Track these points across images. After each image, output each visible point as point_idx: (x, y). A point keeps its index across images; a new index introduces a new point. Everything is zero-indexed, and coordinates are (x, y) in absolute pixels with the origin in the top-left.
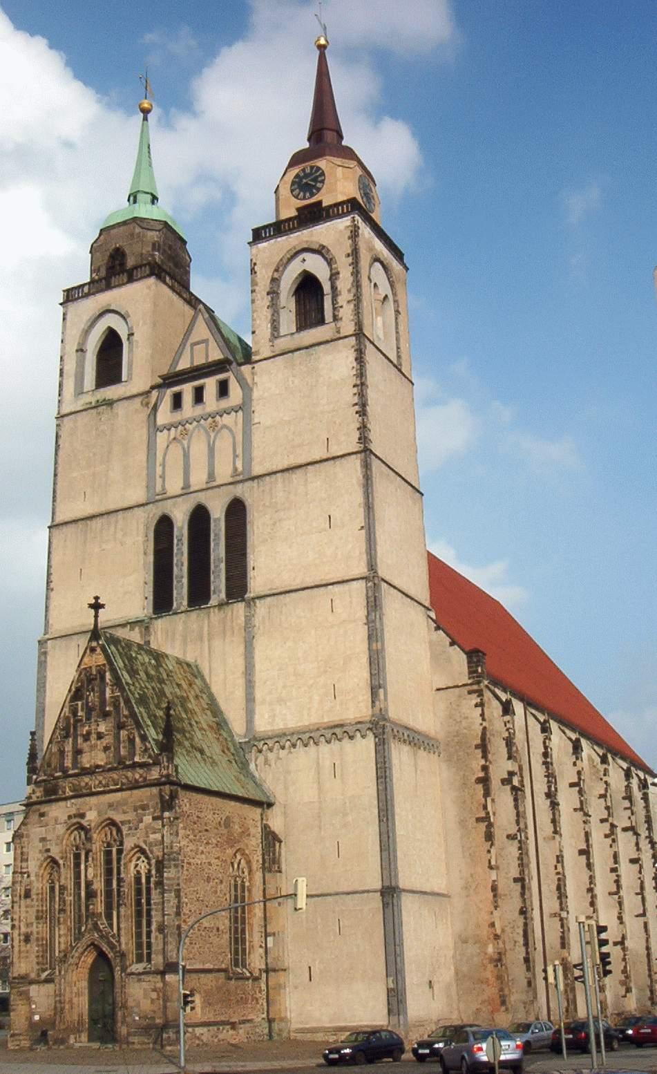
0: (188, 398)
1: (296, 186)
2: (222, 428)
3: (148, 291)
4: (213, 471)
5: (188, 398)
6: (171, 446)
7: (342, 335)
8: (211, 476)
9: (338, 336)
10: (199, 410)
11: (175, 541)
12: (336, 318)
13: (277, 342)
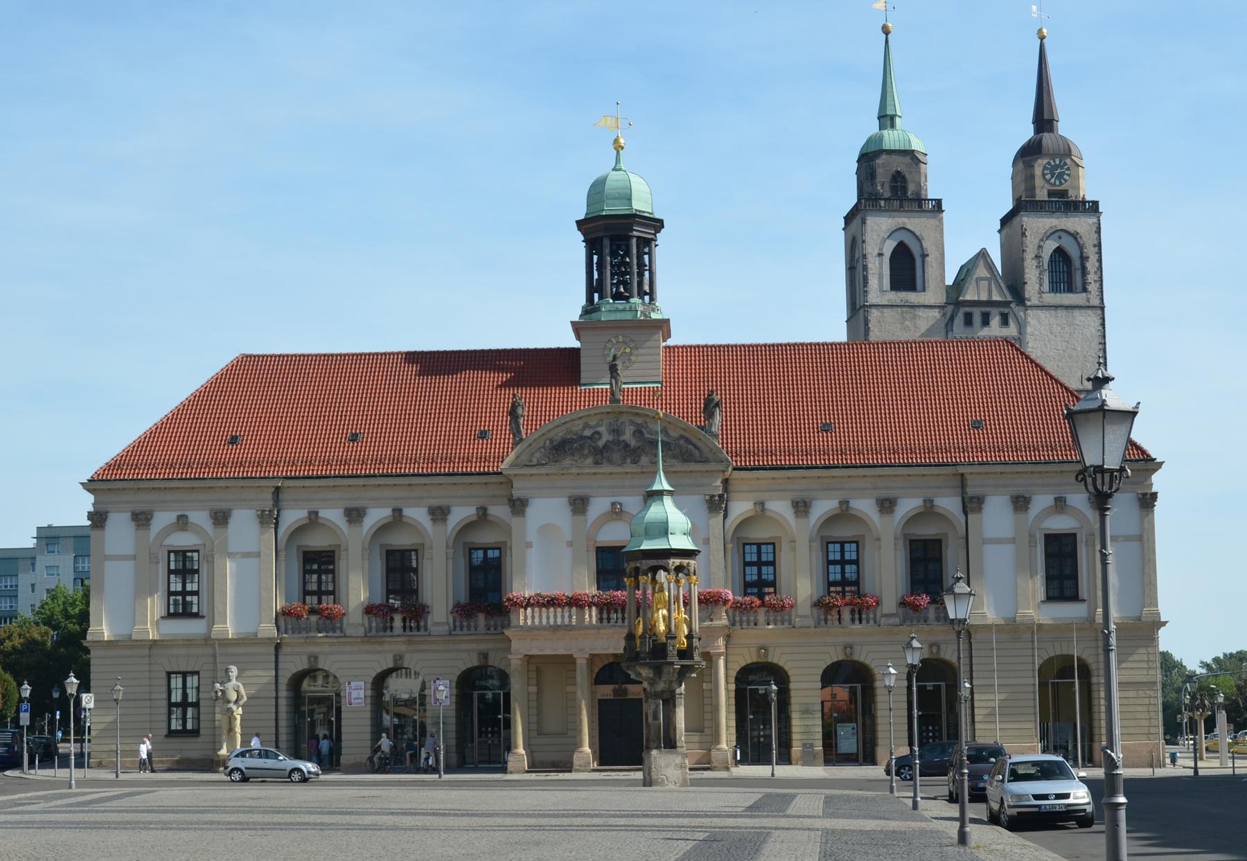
0: (977, 319)
5: (977, 319)
12: (1085, 290)
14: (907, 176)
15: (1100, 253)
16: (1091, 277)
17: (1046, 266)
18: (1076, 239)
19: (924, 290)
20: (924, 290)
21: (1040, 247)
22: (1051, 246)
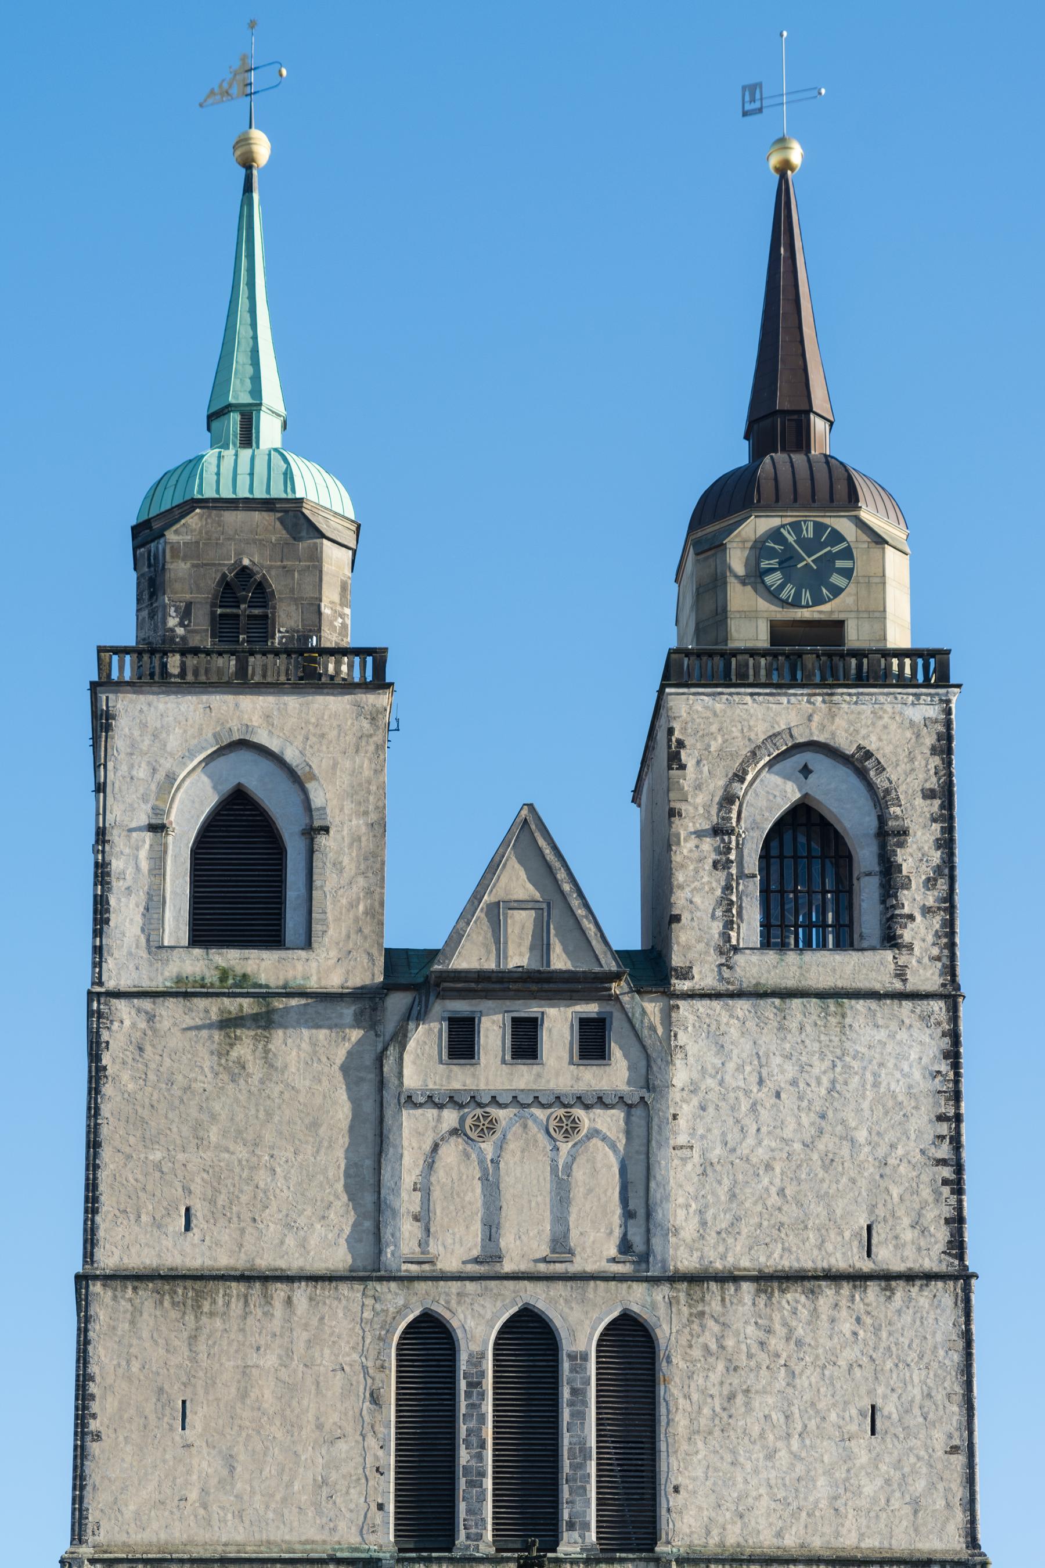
1: (774, 563)
2: (589, 1137)
3: (366, 724)
4: (566, 1235)
6: (443, 1150)
7: (910, 987)
8: (561, 1246)
9: (898, 985)
10: (524, 1077)
11: (463, 1385)
12: (890, 940)
13: (739, 959)
14: (275, 584)
15: (947, 818)
16: (914, 898)
17: (752, 863)
18: (862, 774)
19: (308, 945)
20: (308, 945)
21: (728, 799)
22: (772, 796)
